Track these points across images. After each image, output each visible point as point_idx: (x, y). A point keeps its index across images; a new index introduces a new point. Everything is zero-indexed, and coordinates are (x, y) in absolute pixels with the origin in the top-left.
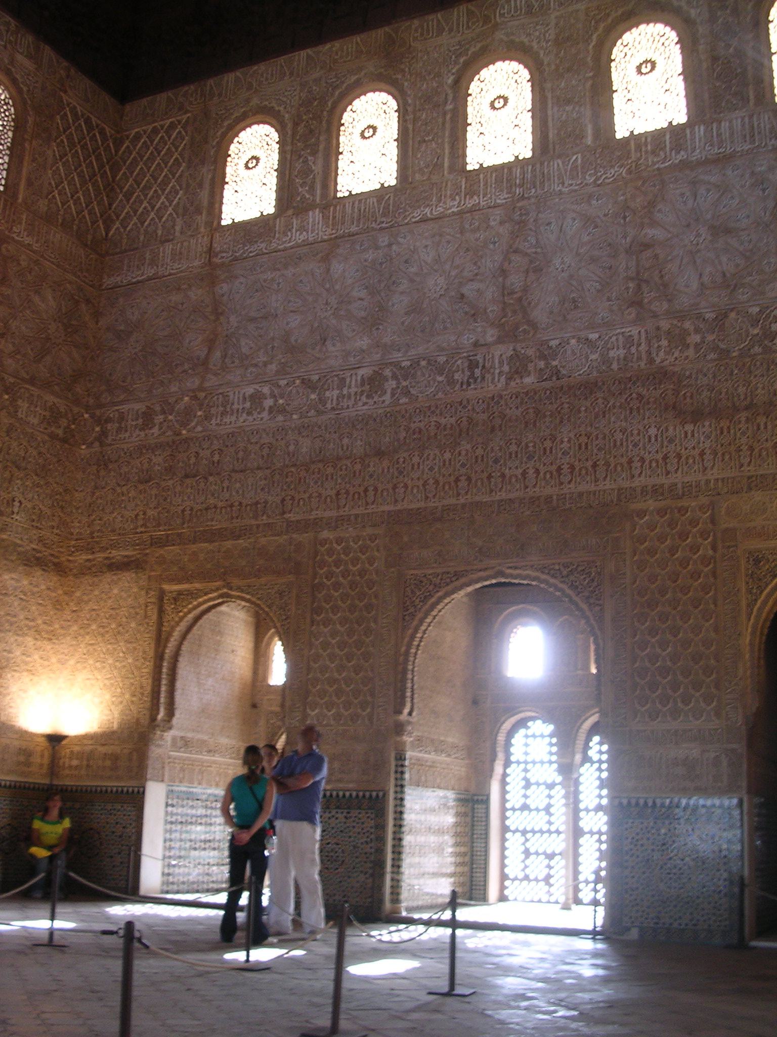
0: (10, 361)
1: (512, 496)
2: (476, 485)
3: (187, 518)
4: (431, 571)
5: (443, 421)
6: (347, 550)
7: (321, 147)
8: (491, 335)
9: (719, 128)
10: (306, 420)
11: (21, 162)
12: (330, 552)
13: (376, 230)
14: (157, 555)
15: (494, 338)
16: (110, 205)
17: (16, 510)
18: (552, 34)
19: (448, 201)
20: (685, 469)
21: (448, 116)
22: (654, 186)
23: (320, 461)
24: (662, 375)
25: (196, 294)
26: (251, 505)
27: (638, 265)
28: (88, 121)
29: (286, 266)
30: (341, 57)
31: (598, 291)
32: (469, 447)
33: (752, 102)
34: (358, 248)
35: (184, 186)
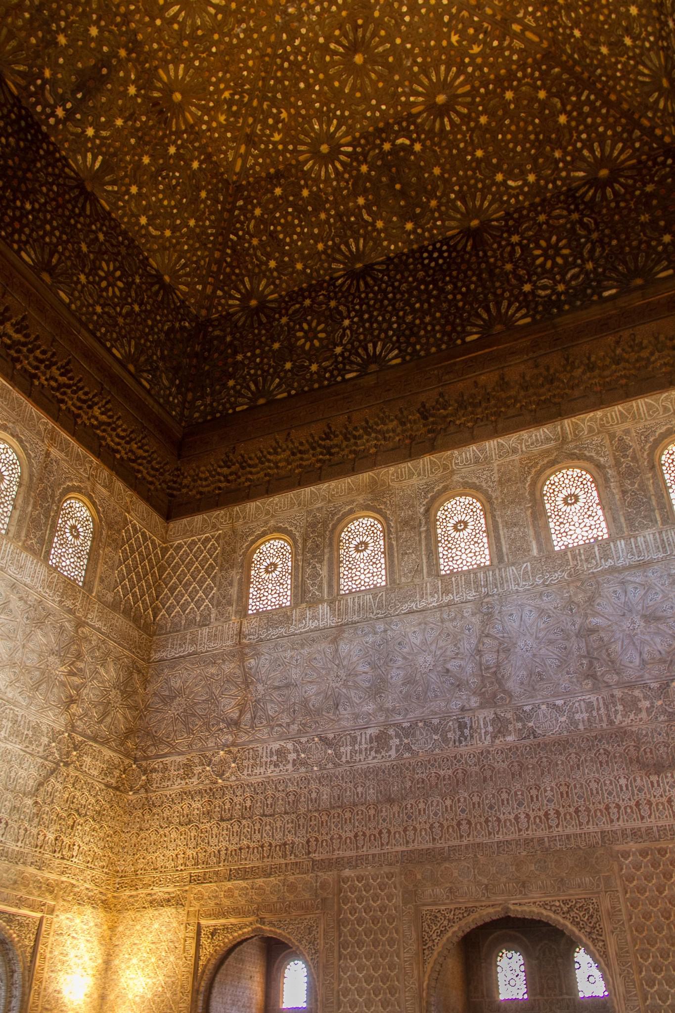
0: (79, 722)
1: (508, 838)
2: (476, 828)
3: (223, 857)
4: (443, 908)
5: (442, 773)
6: (367, 887)
7: (326, 557)
8: (474, 702)
9: (636, 543)
10: (325, 772)
11: (97, 564)
12: (353, 889)
13: (373, 619)
14: (196, 891)
15: (478, 704)
16: (158, 597)
17: (75, 854)
18: (496, 477)
19: (429, 597)
20: (657, 814)
21: (423, 535)
22: (592, 585)
23: (338, 807)
24: (621, 734)
25: (229, 667)
26: (280, 846)
27: (587, 646)
28: (144, 534)
29: (302, 646)
30: (337, 493)
31: (558, 667)
32: (466, 795)
33: (659, 523)
34: (360, 632)
35: (217, 584)
